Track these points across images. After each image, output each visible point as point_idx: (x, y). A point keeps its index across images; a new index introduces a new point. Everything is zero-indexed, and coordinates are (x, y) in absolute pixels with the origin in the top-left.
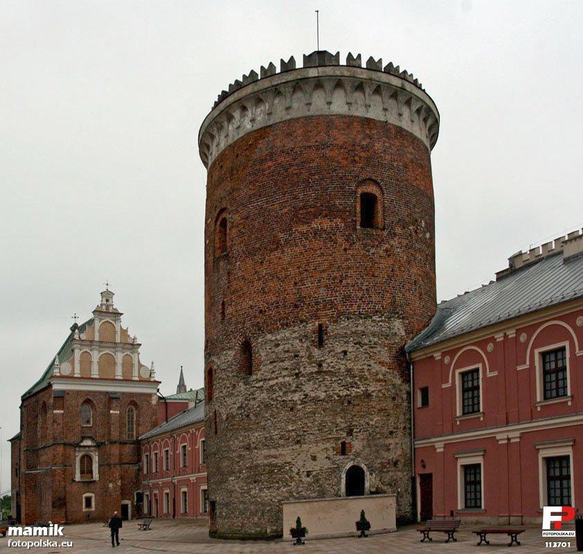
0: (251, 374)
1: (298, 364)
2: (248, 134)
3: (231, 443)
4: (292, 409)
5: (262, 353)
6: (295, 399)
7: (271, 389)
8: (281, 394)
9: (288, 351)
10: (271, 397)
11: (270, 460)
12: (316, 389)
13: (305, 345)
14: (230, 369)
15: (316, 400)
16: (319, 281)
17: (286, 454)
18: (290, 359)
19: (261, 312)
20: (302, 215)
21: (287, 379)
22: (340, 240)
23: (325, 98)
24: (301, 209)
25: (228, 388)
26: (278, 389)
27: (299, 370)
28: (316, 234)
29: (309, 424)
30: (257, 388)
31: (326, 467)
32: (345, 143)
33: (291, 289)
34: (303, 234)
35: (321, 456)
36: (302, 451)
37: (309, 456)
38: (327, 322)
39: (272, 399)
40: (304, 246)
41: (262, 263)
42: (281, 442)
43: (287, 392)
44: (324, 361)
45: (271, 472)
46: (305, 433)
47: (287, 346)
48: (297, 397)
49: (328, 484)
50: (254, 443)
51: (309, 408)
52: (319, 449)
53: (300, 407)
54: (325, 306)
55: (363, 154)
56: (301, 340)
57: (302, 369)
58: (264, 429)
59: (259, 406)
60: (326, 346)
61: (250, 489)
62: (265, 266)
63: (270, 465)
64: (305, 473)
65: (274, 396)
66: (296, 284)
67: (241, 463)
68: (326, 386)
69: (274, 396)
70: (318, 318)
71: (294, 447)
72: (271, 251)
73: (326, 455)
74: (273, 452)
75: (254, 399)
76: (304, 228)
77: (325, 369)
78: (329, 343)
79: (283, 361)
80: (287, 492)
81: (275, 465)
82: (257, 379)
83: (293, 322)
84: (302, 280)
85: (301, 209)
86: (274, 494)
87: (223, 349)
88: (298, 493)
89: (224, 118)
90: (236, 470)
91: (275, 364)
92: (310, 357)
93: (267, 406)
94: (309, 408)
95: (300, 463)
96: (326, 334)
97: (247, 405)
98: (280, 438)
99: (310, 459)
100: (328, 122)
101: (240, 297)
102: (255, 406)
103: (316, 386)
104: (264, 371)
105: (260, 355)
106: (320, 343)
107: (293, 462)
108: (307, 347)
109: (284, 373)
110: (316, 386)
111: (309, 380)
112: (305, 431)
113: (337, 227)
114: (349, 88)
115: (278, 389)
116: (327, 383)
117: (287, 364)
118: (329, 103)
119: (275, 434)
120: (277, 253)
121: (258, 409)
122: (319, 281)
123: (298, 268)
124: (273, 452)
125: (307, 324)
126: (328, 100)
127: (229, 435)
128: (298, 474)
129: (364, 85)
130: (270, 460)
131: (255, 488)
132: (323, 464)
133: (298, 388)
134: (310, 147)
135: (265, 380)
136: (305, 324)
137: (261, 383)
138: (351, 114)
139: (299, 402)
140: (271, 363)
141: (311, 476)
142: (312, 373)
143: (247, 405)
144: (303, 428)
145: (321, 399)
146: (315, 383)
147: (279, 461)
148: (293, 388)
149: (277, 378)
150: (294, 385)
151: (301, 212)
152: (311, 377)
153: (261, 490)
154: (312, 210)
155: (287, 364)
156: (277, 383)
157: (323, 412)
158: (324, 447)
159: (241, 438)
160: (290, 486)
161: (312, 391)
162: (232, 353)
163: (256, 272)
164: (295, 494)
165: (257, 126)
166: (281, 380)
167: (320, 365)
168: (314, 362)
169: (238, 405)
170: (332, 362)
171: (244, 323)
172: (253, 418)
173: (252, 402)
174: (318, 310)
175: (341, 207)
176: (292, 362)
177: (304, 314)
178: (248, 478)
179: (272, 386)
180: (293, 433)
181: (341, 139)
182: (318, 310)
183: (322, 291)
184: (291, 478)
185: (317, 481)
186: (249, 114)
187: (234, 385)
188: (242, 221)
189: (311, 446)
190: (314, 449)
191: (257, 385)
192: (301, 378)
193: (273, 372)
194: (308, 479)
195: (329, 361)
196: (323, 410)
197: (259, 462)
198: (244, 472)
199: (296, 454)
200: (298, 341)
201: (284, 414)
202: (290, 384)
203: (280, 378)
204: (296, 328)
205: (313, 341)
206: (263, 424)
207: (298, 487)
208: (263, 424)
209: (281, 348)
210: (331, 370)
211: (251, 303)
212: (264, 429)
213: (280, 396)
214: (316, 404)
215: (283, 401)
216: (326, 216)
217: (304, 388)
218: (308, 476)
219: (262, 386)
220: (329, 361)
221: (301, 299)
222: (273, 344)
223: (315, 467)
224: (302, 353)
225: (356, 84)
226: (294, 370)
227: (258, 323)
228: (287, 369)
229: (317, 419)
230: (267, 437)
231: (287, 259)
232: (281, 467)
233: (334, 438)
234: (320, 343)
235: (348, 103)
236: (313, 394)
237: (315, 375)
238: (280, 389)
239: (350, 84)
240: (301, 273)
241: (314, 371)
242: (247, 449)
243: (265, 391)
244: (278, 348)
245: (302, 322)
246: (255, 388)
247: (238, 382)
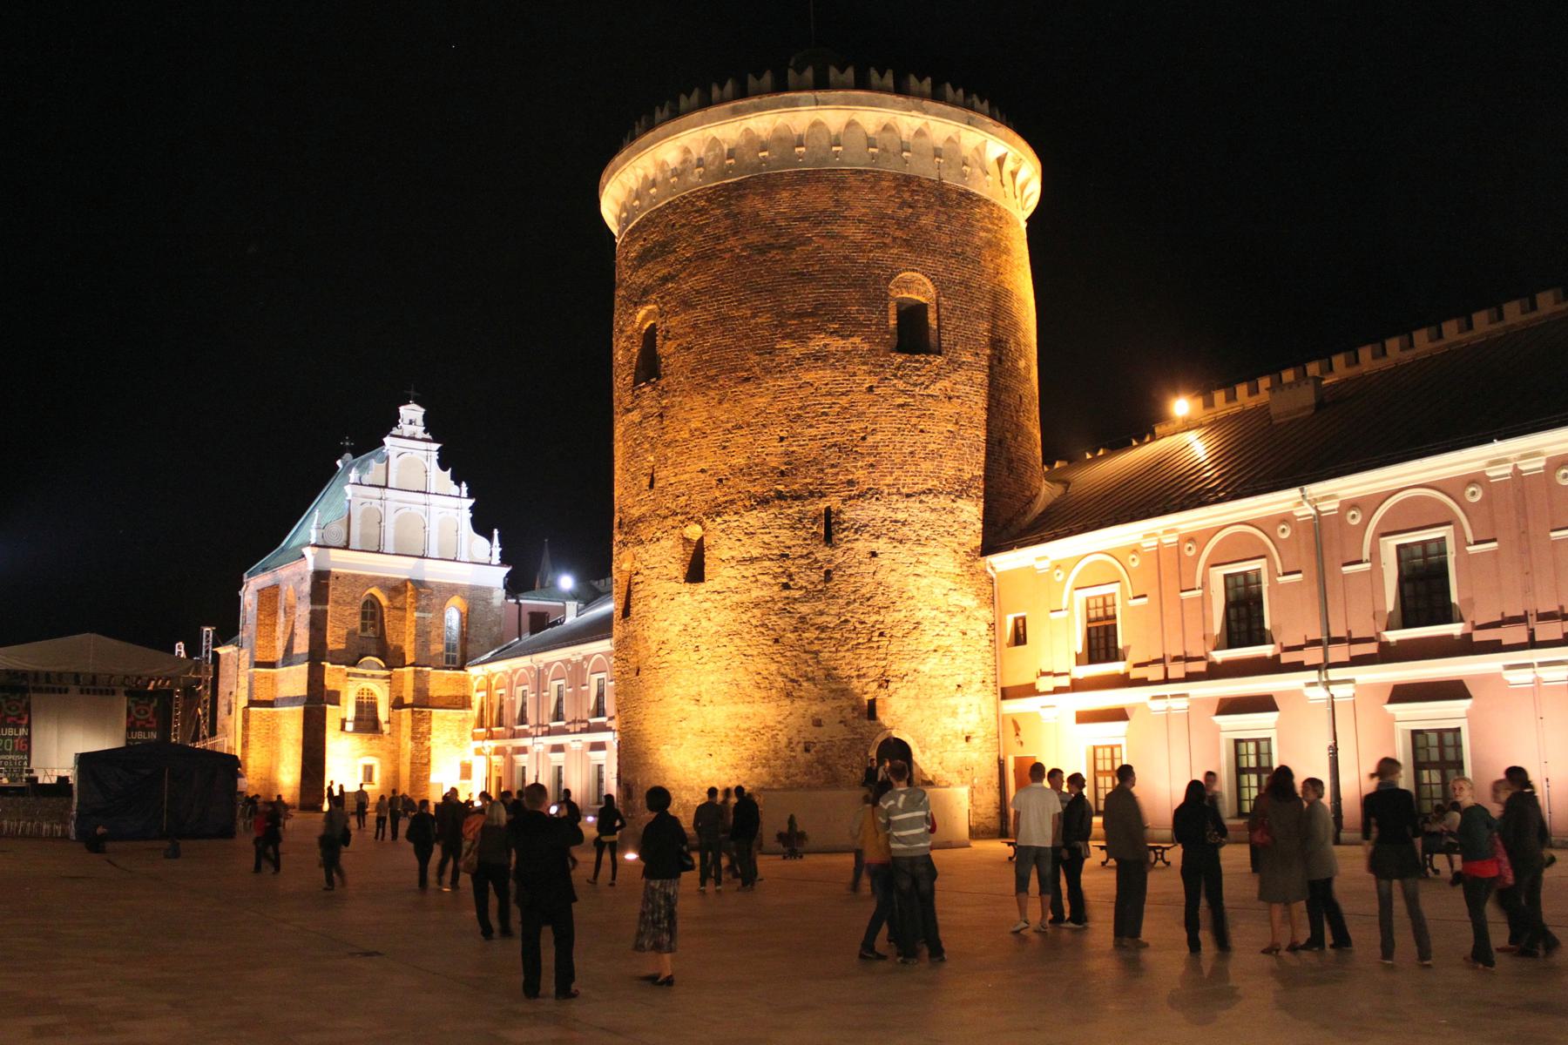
55: (898, 233)
101: (682, 453)
113: (855, 349)
194: (808, 756)
218: (807, 750)
234: (828, 539)
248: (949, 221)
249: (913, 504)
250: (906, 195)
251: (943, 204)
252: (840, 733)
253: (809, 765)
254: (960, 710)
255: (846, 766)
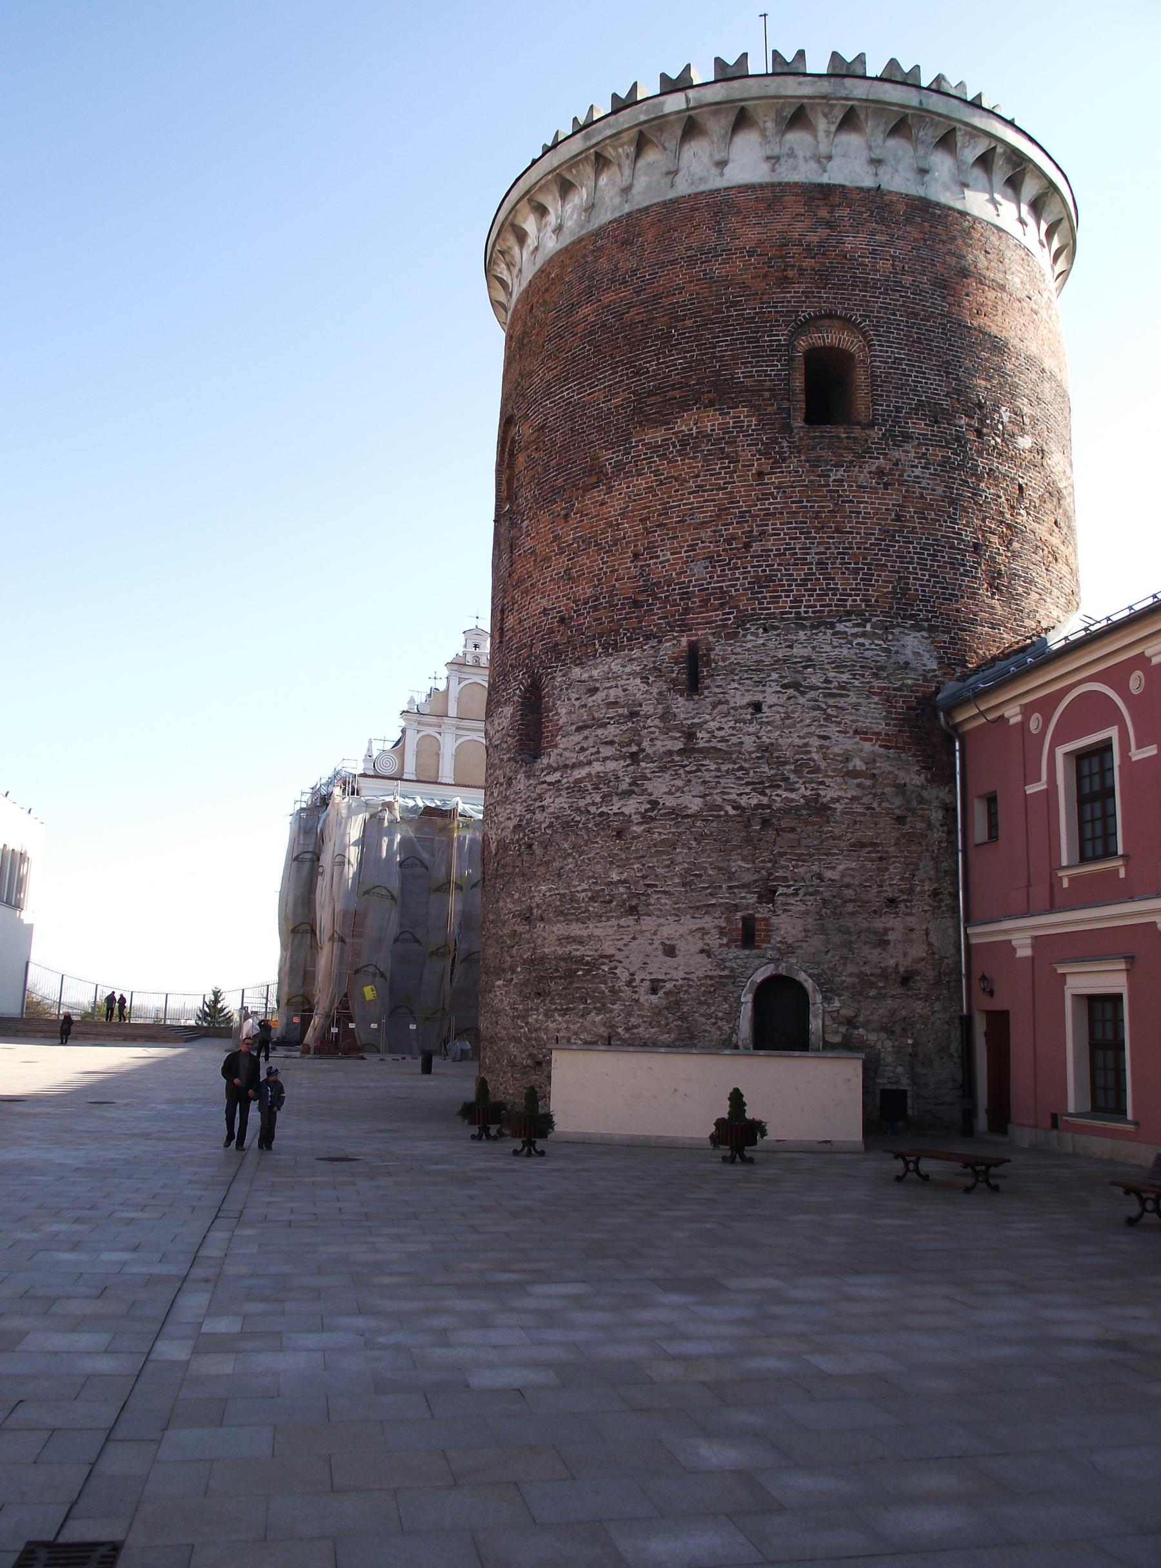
0: (536, 756)
1: (636, 732)
2: (551, 260)
3: (501, 904)
4: (619, 834)
5: (563, 711)
6: (626, 811)
7: (576, 788)
8: (598, 799)
9: (615, 703)
10: (575, 805)
11: (569, 948)
12: (678, 789)
13: (655, 691)
14: (505, 746)
15: (677, 814)
16: (692, 548)
17: (603, 935)
18: (619, 720)
19: (562, 620)
20: (655, 405)
21: (611, 765)
22: (746, 455)
23: (711, 155)
24: (651, 394)
25: (501, 784)
26: (590, 787)
27: (639, 745)
28: (684, 444)
29: (659, 871)
30: (550, 784)
31: (700, 973)
32: (760, 242)
33: (627, 567)
34: (653, 447)
35: (689, 947)
36: (642, 932)
37: (657, 943)
38: (711, 638)
39: (578, 809)
40: (657, 473)
41: (566, 516)
42: (594, 907)
43: (610, 795)
44: (700, 725)
45: (570, 974)
46: (650, 891)
47: (612, 692)
48: (631, 806)
49: (701, 1015)
50: (538, 906)
51: (663, 831)
52: (682, 930)
53: (638, 829)
54: (705, 602)
56: (645, 679)
57: (645, 744)
58: (559, 875)
59: (551, 826)
60: (706, 692)
61: (527, 1010)
62: (573, 523)
63: (568, 958)
64: (647, 984)
65: (582, 803)
66: (636, 556)
67: (514, 951)
68: (704, 782)
69: (582, 803)
70: (686, 628)
71: (622, 922)
72: (586, 490)
73: (700, 945)
74: (576, 929)
75: (543, 808)
76: (656, 435)
77: (702, 744)
78: (713, 687)
79: (604, 725)
80: (604, 1025)
81: (580, 960)
82: (549, 766)
83: (630, 639)
84: (651, 548)
85: (651, 394)
86: (575, 1027)
87: (499, 704)
88: (627, 1030)
89: (511, 241)
90: (507, 965)
91: (586, 732)
92: (666, 716)
93: (568, 826)
94: (663, 831)
95: (636, 960)
96: (708, 664)
97: (529, 822)
98: (593, 899)
99: (660, 952)
100: (720, 206)
101: (526, 592)
102: (544, 826)
103: (679, 783)
104: (565, 746)
105: (557, 714)
106: (693, 685)
107: (619, 956)
108: (660, 693)
109: (607, 751)
110: (679, 783)
111: (663, 769)
112: (648, 886)
113: (738, 425)
114: (770, 125)
115: (590, 787)
116: (707, 776)
117: (611, 731)
118: (722, 164)
119: (582, 888)
120: (598, 494)
121: (549, 831)
122: (692, 548)
123: (643, 521)
124: (576, 929)
125: (660, 642)
126: (717, 157)
127: (499, 886)
128: (629, 983)
129: (809, 113)
130: (569, 948)
131: (537, 1010)
132: (689, 964)
133: (637, 786)
134: (673, 262)
135: (566, 766)
136: (654, 642)
137: (556, 776)
138: (776, 179)
139: (636, 818)
140: (579, 729)
141: (661, 993)
142: (670, 753)
143: (529, 822)
144: (644, 877)
145: (689, 812)
146: (677, 775)
147: (586, 952)
148: (624, 786)
149: (590, 763)
150: (628, 780)
151: (651, 400)
152: (666, 762)
153: (548, 1014)
154: (677, 394)
155: (611, 731)
156: (589, 774)
157: (694, 844)
158: (694, 924)
159: (516, 896)
160: (612, 1011)
161: (670, 793)
162: (508, 710)
163: (556, 538)
164: (620, 1030)
165: (566, 239)
166: (597, 767)
167: (690, 736)
168: (676, 728)
169: (515, 822)
170: (720, 729)
171: (531, 647)
172: (538, 850)
173: (539, 816)
174: (687, 610)
175: (749, 382)
176: (624, 728)
177: (656, 620)
178: (526, 983)
179: (578, 781)
180: (622, 890)
181: (750, 235)
182: (687, 610)
183: (699, 570)
184: (614, 991)
185: (678, 1003)
186: (552, 219)
187: (510, 778)
188: (532, 438)
189: (662, 920)
190: (670, 930)
191: (549, 779)
192: (643, 764)
193: (583, 749)
194: (654, 999)
195: (713, 725)
196: (696, 839)
197: (546, 951)
198: (519, 969)
199: (627, 938)
200: (638, 681)
201: (602, 845)
202: (617, 778)
203: (595, 764)
204: (636, 653)
205: (673, 680)
206: (556, 864)
207: (630, 1014)
208: (556, 864)
209: (600, 696)
210: (719, 745)
211: (544, 602)
212: (559, 875)
213: (593, 804)
214: (677, 825)
215: (602, 814)
216: (711, 404)
217: (648, 785)
218: (654, 991)
219: (559, 781)
220: (714, 726)
221: (650, 589)
222: (583, 688)
223: (673, 971)
224: (647, 708)
225: (788, 113)
226: (629, 745)
227: (557, 644)
228: (612, 743)
229: (680, 859)
230: (564, 895)
231: (617, 505)
232: (592, 965)
233: (720, 905)
234: (693, 685)
235: (769, 158)
236: (670, 802)
237: (677, 758)
238: (597, 788)
239: (772, 115)
240: (648, 532)
241: (676, 748)
242: (527, 919)
243: (564, 793)
244: (594, 698)
245: (647, 638)
246: (545, 786)
247: (516, 772)
248: (890, 243)
249: (824, 637)
250: (823, 213)
251: (882, 221)
252: (702, 967)
253: (658, 1012)
254: (891, 936)
255: (708, 1016)
